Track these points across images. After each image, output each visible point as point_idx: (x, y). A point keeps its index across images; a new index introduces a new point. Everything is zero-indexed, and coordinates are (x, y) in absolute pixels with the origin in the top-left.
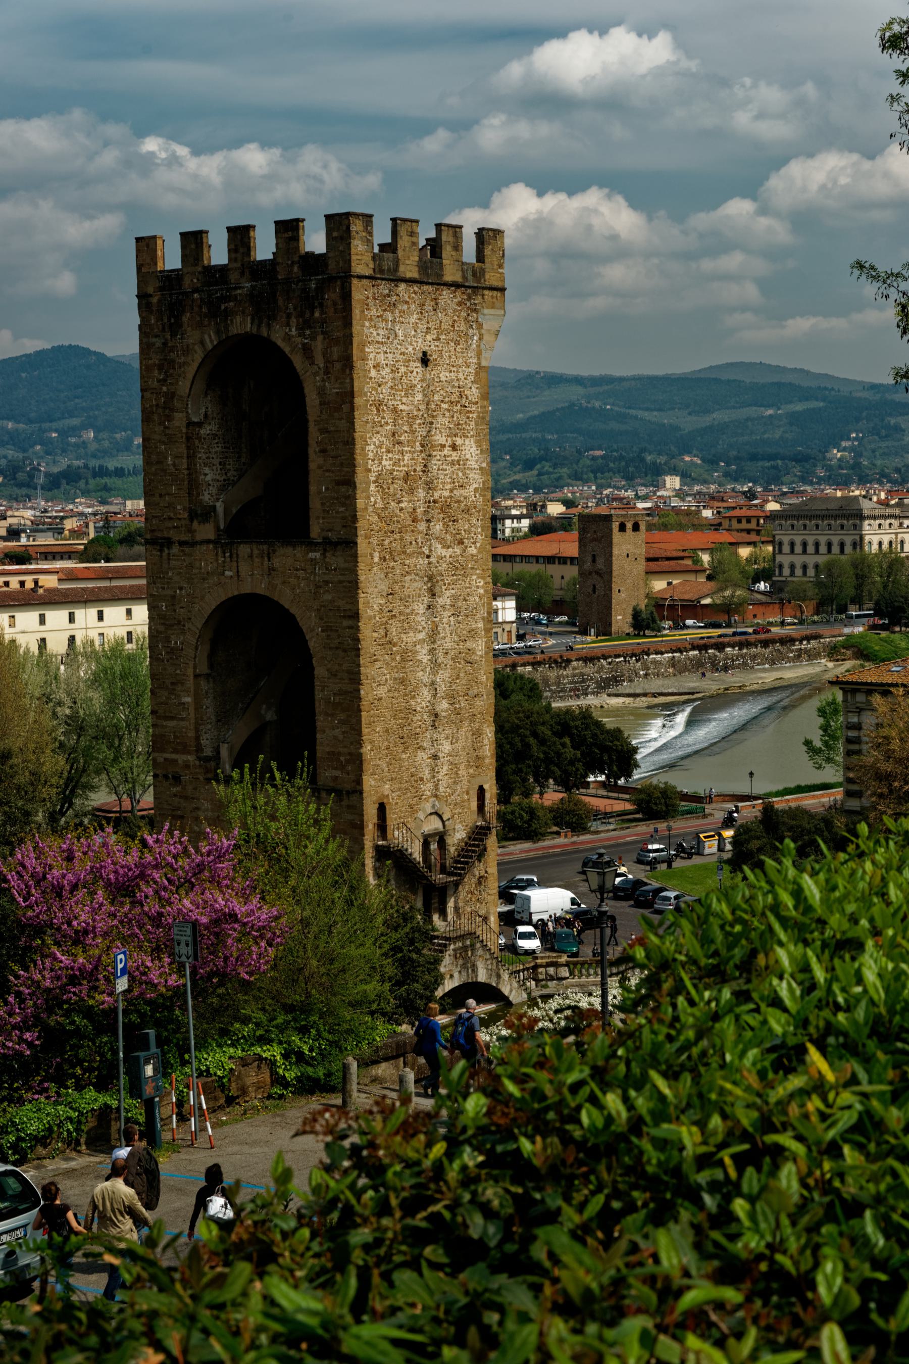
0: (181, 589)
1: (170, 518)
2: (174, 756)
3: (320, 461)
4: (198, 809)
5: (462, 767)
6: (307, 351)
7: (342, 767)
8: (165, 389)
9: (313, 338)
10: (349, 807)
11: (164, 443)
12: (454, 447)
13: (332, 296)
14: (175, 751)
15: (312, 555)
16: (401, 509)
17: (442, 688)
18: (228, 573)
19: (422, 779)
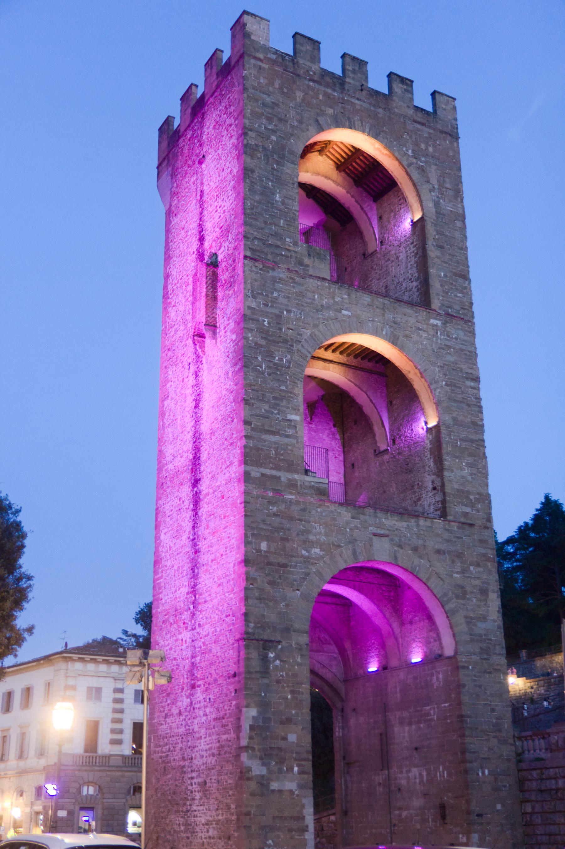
0: (289, 311)
2: (274, 473)
3: (438, 253)
4: (307, 532)
7: (472, 505)
8: (274, 138)
10: (481, 541)
11: (272, 181)
14: (278, 468)
15: (432, 321)
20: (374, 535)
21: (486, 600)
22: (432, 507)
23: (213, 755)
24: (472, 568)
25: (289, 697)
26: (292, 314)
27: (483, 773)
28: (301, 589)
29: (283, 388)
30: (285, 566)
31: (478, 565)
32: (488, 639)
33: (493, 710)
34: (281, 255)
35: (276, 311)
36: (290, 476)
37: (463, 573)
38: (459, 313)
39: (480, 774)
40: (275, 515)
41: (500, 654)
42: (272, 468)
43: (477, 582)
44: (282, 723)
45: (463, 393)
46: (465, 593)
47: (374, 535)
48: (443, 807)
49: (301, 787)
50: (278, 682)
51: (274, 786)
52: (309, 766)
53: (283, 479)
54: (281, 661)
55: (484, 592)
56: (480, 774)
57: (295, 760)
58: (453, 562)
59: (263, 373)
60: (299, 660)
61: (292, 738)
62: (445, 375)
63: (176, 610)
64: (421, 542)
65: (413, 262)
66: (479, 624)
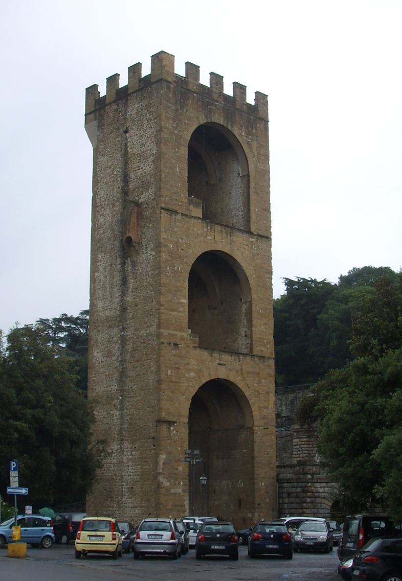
0: (182, 239)
1: (177, 200)
2: (174, 332)
4: (188, 364)
6: (249, 144)
9: (253, 140)
13: (260, 125)
14: (176, 330)
15: (251, 239)
18: (208, 237)
20: (219, 364)
22: (244, 346)
23: (138, 475)
24: (263, 380)
25: (179, 449)
26: (184, 241)
27: (262, 484)
28: (186, 394)
29: (179, 284)
30: (178, 382)
31: (266, 379)
33: (268, 454)
34: (179, 205)
35: (176, 240)
39: (260, 485)
40: (174, 355)
41: (273, 426)
42: (173, 330)
46: (259, 394)
47: (219, 364)
48: (240, 500)
49: (184, 491)
50: (175, 442)
51: (172, 491)
52: (187, 482)
53: (178, 336)
54: (176, 431)
55: (268, 393)
56: (260, 485)
57: (182, 479)
59: (169, 277)
60: (184, 430)
61: (180, 468)
62: (256, 271)
63: (108, 397)
64: (240, 367)
65: (240, 199)
66: (265, 410)
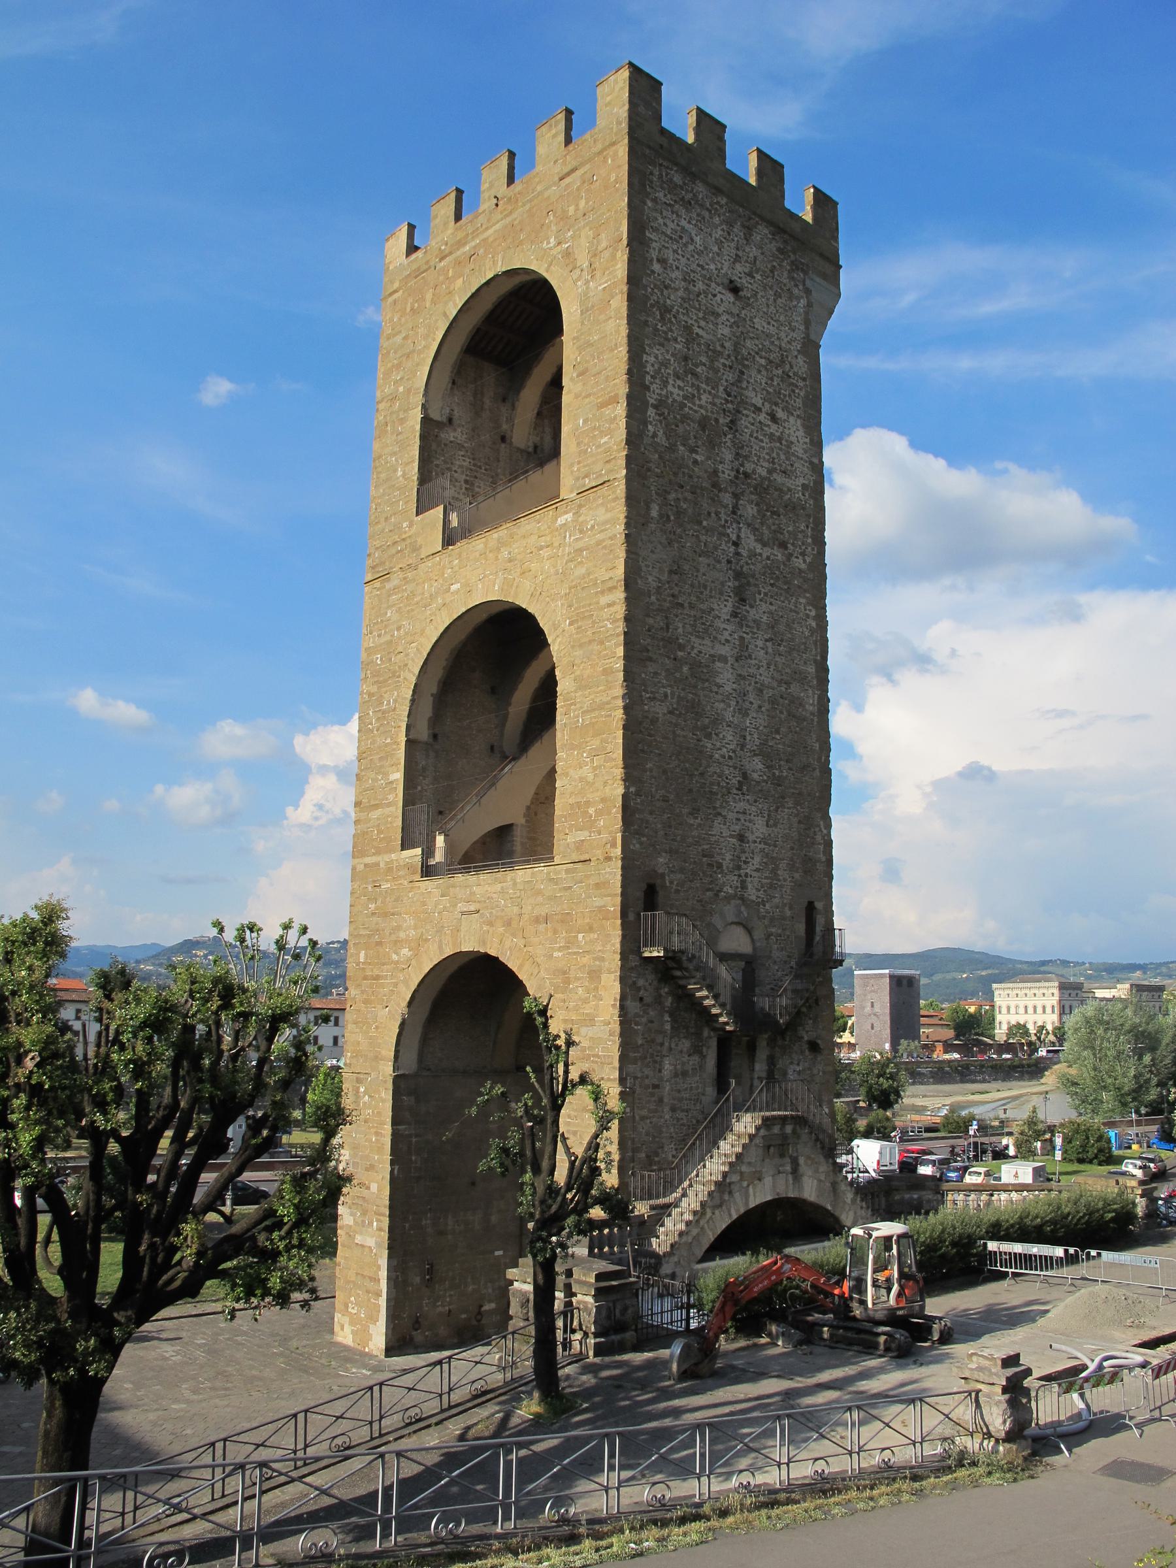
4: (399, 928)
5: (783, 865)
12: (774, 418)
14: (378, 852)
16: (696, 462)
17: (753, 741)
19: (720, 866)
21: (596, 989)
29: (389, 741)
30: (377, 978)
31: (591, 929)
32: (594, 1056)
36: (386, 858)
37: (568, 948)
38: (601, 475)
43: (585, 960)
44: (367, 1170)
45: (594, 622)
49: (378, 1245)
55: (594, 975)
58: (555, 932)
